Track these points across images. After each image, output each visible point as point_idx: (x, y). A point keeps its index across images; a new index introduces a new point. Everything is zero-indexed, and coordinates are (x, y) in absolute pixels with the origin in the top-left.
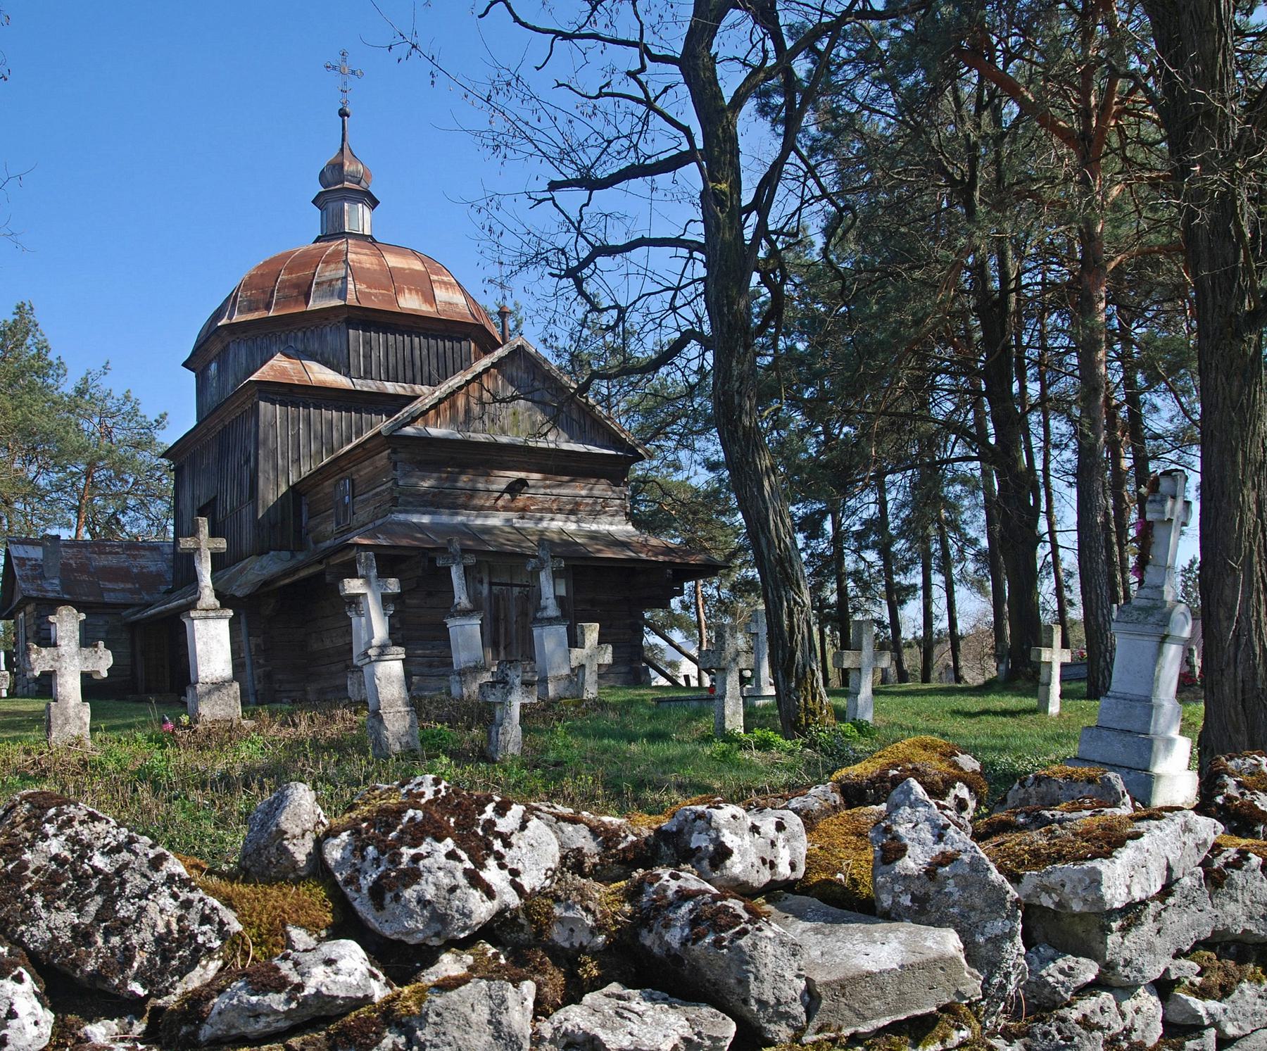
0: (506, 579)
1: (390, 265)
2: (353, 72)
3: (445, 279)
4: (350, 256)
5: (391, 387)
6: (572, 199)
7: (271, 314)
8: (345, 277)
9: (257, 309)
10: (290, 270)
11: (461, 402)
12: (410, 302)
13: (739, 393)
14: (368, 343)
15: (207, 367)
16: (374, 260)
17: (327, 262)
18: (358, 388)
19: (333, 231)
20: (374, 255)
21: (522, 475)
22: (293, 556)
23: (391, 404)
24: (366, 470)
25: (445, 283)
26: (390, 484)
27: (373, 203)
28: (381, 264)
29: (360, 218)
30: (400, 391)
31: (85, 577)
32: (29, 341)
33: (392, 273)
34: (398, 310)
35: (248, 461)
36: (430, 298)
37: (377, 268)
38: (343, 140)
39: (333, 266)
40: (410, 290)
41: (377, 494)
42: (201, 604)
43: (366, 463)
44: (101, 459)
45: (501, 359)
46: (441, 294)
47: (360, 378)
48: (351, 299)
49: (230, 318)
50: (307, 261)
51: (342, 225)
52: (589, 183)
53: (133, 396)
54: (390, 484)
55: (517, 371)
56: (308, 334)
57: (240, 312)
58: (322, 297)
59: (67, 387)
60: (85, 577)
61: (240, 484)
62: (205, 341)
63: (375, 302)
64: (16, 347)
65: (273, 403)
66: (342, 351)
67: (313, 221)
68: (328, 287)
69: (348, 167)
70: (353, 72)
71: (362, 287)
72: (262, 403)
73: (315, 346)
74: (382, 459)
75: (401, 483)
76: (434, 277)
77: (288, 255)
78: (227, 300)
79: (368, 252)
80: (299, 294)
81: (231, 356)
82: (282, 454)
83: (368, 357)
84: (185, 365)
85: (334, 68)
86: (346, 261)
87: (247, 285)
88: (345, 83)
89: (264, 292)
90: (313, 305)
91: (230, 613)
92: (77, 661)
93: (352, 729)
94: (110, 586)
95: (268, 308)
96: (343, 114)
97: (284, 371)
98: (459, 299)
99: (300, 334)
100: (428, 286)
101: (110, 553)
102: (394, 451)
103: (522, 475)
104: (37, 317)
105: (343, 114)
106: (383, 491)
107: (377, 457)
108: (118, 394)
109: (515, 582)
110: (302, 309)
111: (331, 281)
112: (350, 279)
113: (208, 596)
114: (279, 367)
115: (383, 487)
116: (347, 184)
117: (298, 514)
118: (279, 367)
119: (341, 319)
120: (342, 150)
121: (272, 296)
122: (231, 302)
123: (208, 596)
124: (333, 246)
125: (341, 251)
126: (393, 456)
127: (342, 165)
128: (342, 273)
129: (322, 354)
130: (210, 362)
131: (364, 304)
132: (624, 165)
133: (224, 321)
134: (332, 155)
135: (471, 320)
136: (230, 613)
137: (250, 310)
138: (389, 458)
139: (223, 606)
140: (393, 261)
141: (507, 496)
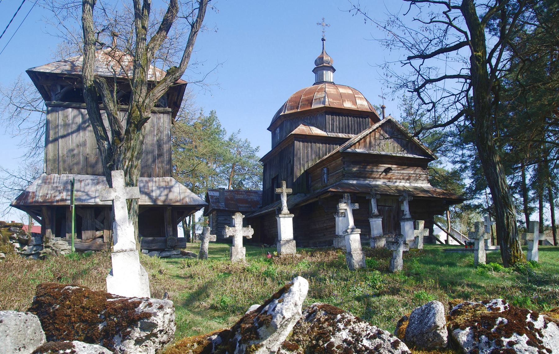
0: (383, 204)
1: (341, 92)
2: (327, 25)
3: (360, 96)
4: (326, 89)
5: (341, 135)
6: (417, 62)
7: (299, 110)
8: (325, 97)
9: (294, 109)
10: (305, 95)
11: (368, 140)
12: (348, 105)
13: (487, 133)
14: (333, 120)
15: (276, 130)
16: (335, 90)
17: (318, 92)
18: (329, 136)
19: (320, 81)
20: (335, 88)
21: (390, 166)
22: (306, 195)
23: (341, 141)
24: (333, 164)
25: (360, 98)
26: (342, 169)
27: (334, 70)
28: (337, 92)
29: (329, 76)
30: (344, 136)
31: (233, 202)
32: (214, 123)
33: (341, 95)
34: (344, 108)
35: (290, 162)
36: (355, 103)
37: (336, 93)
38: (323, 49)
39: (320, 93)
40: (348, 100)
41: (337, 173)
42: (283, 212)
43: (333, 162)
44: (237, 162)
45: (383, 124)
46: (359, 102)
47: (330, 132)
48: (327, 104)
49: (284, 112)
50: (311, 92)
51: (323, 79)
52: (424, 56)
53: (248, 140)
54: (342, 169)
55: (388, 129)
57: (288, 110)
58: (317, 104)
59: (226, 138)
60: (233, 202)
62: (275, 121)
63: (336, 104)
64: (210, 125)
65: (299, 141)
66: (323, 123)
67: (312, 78)
68: (319, 100)
69: (325, 58)
70: (327, 25)
71: (331, 100)
72: (296, 142)
73: (314, 121)
74: (339, 161)
75: (346, 169)
76: (356, 96)
77: (304, 90)
78: (283, 106)
79: (333, 87)
80: (309, 103)
81: (284, 125)
83: (333, 125)
84: (268, 129)
85: (320, 24)
86: (325, 91)
87: (290, 101)
89: (296, 103)
90: (314, 107)
91: (293, 215)
92: (241, 232)
93: (336, 258)
94: (241, 205)
95: (297, 108)
96: (323, 40)
97: (303, 130)
98: (365, 103)
99: (309, 117)
100: (354, 99)
101: (241, 194)
102: (344, 158)
103: (390, 166)
104: (217, 115)
105: (323, 40)
106: (339, 172)
107: (337, 160)
108: (243, 140)
109: (387, 205)
110: (310, 108)
111: (320, 98)
112: (326, 97)
113: (285, 210)
114: (301, 129)
115: (339, 171)
116: (325, 64)
118: (301, 129)
119: (323, 111)
120: (323, 52)
121: (299, 104)
122: (284, 107)
123: (285, 210)
124: (320, 86)
125: (323, 88)
127: (323, 58)
128: (324, 95)
130: (277, 128)
131: (332, 106)
132: (438, 48)
133: (282, 114)
134: (319, 54)
135: (370, 111)
136: (293, 215)
137: (291, 109)
138: (342, 160)
139: (291, 213)
140: (342, 90)
141: (384, 174)
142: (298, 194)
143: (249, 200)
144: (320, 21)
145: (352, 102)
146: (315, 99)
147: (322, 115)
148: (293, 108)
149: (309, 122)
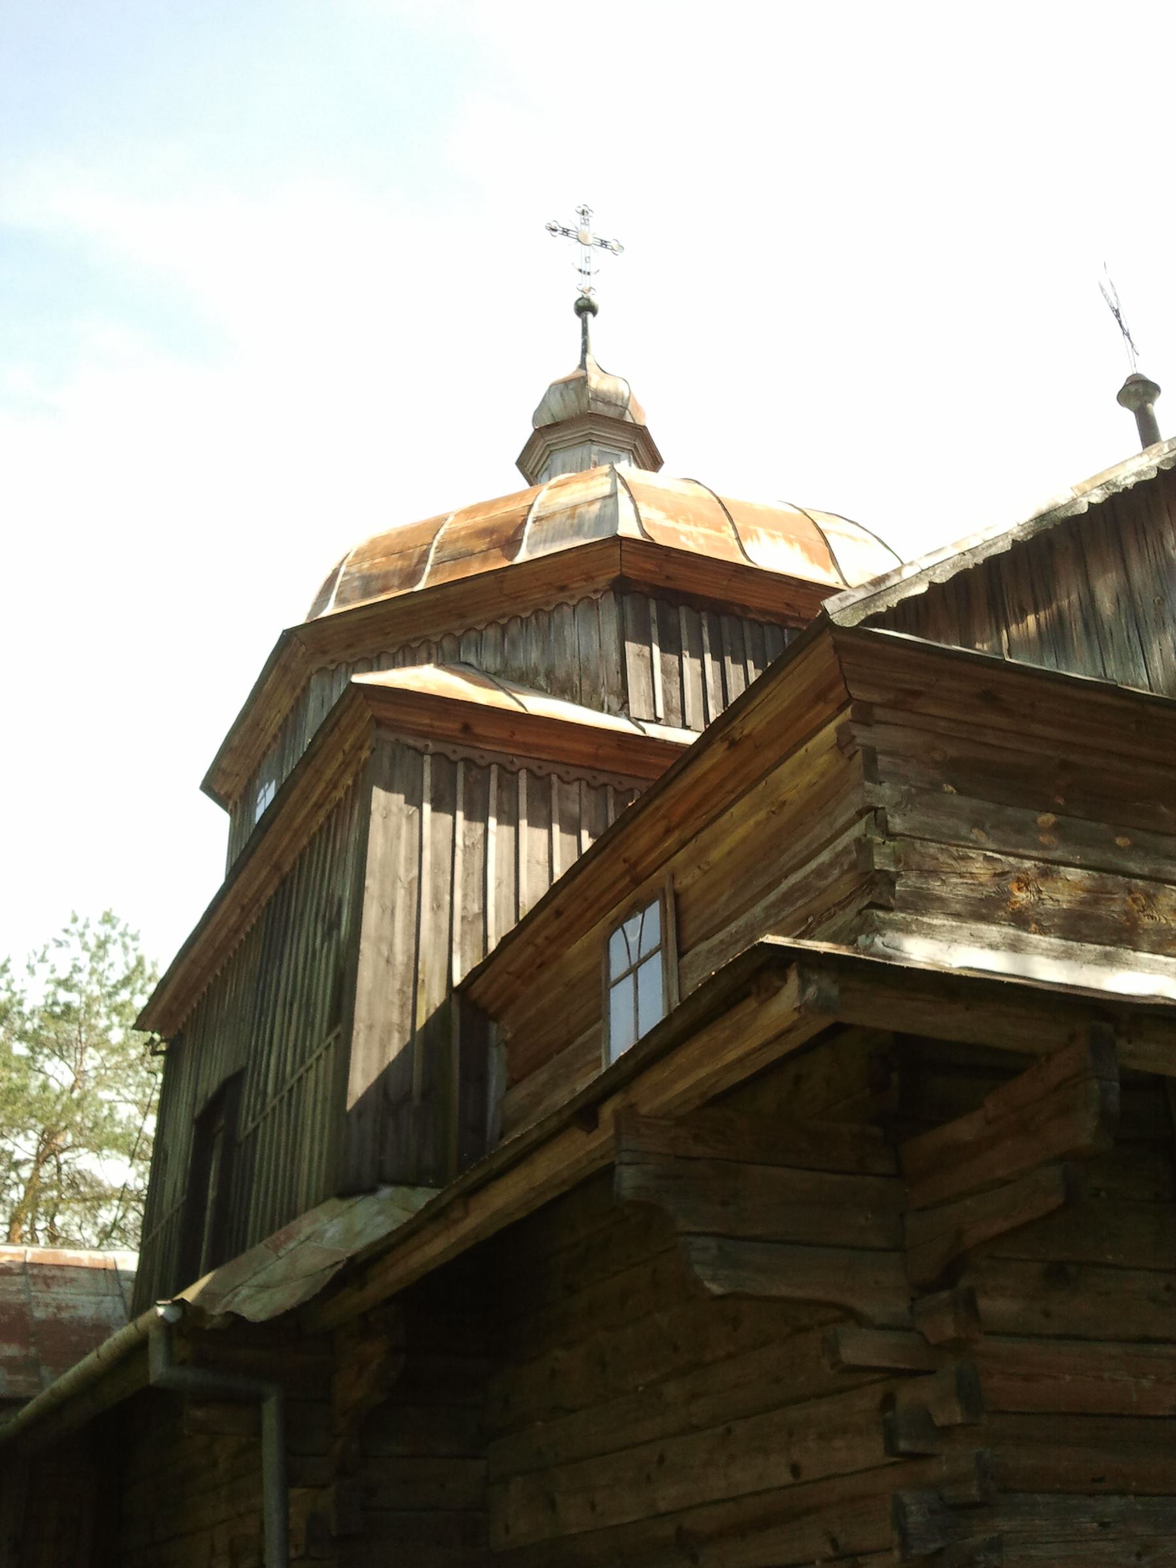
2: (604, 244)
8: (613, 495)
35: (335, 924)
38: (585, 351)
54: (856, 831)
56: (514, 629)
61: (308, 1005)
66: (603, 657)
70: (604, 244)
82: (436, 897)
85: (566, 232)
88: (587, 259)
105: (585, 308)
111: (575, 507)
115: (825, 857)
117: (476, 1075)
119: (603, 581)
126: (862, 736)
128: (607, 490)
129: (549, 674)
137: (366, 594)
142: (386, 1192)
143: (39, 1314)
144: (572, 221)
145: (806, 548)
146: (538, 520)
147: (593, 605)
148: (379, 584)
149: (490, 661)
